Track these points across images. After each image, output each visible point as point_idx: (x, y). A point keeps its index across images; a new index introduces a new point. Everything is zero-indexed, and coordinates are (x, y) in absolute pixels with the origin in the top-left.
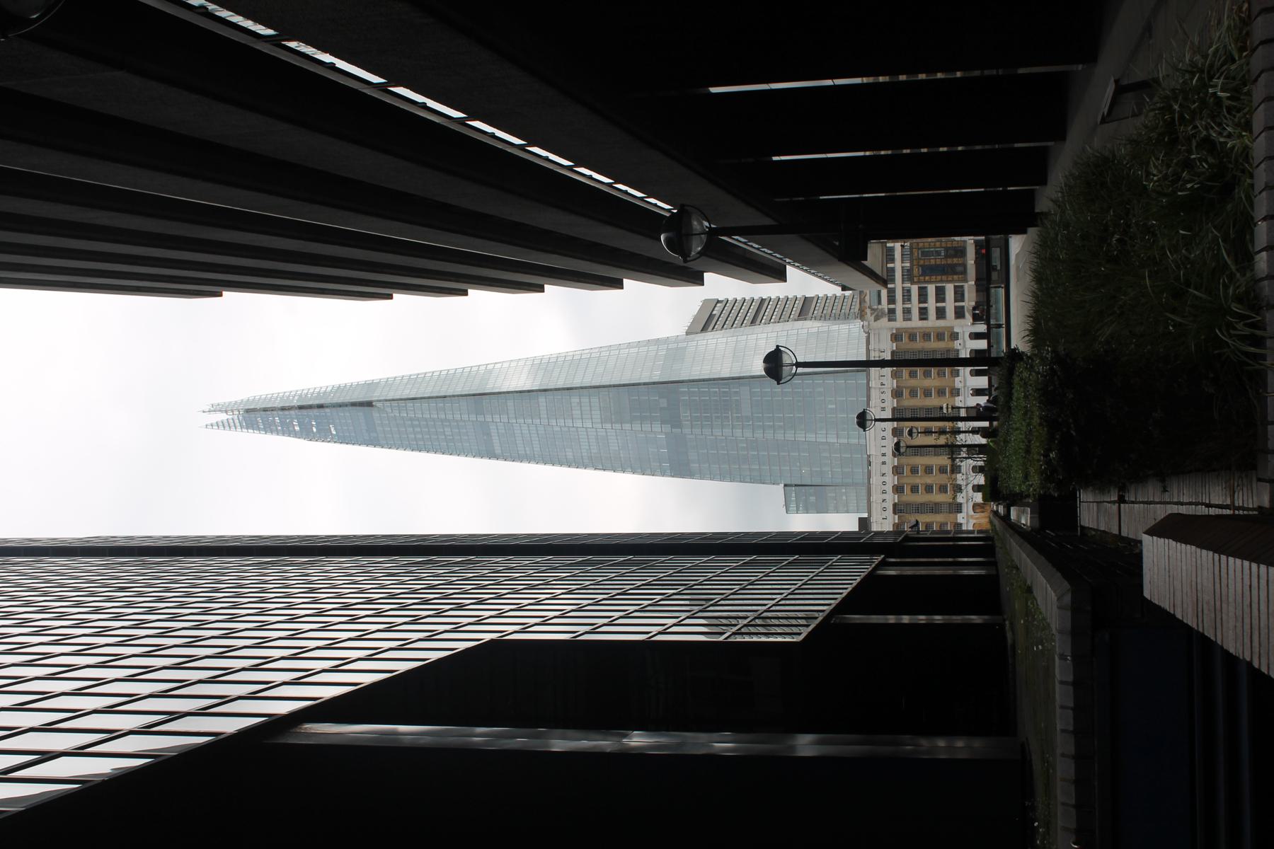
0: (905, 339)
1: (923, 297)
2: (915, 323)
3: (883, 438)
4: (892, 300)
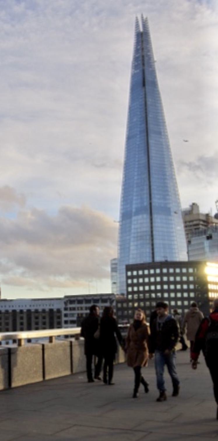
0: (58, 314)
2: (64, 319)
3: (19, 306)
4: (71, 309)
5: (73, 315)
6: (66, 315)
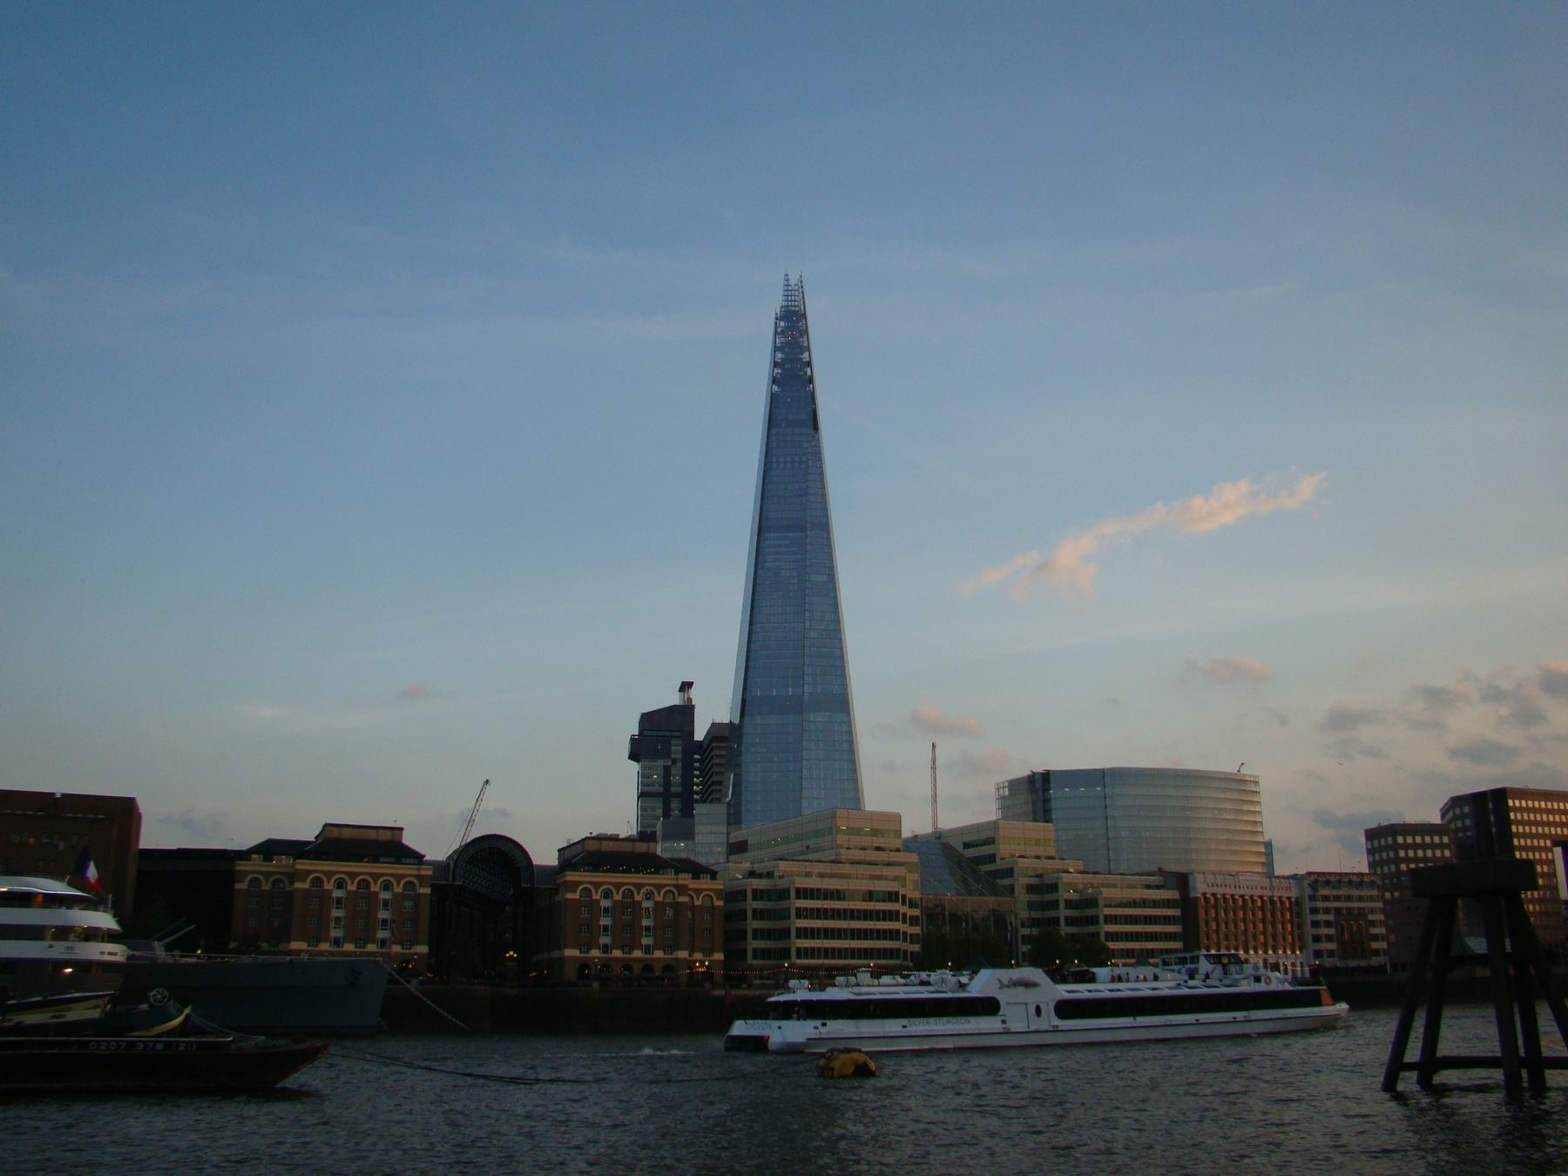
1: (1328, 924)
4: (1326, 898)
5: (1327, 911)
6: (1314, 911)
